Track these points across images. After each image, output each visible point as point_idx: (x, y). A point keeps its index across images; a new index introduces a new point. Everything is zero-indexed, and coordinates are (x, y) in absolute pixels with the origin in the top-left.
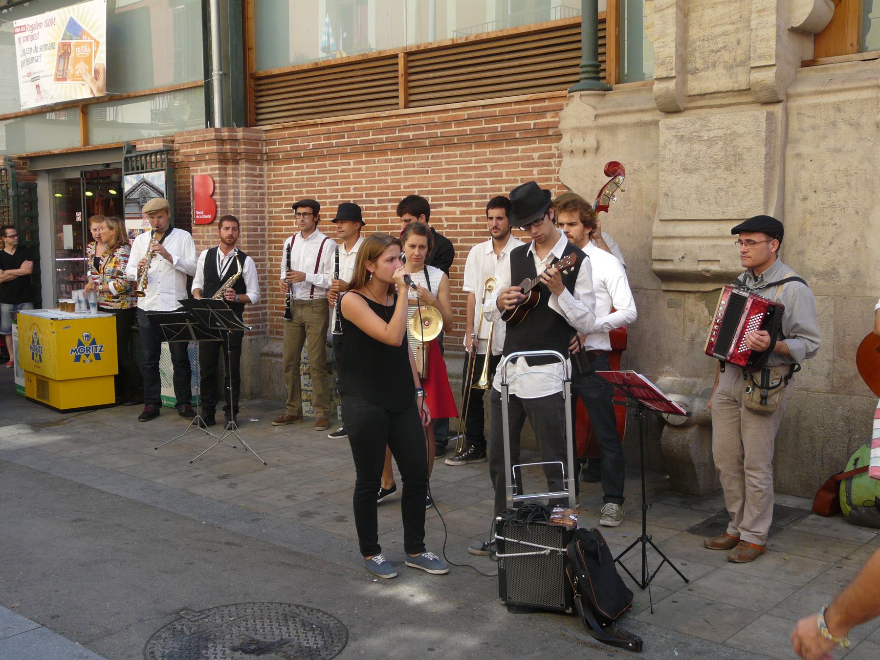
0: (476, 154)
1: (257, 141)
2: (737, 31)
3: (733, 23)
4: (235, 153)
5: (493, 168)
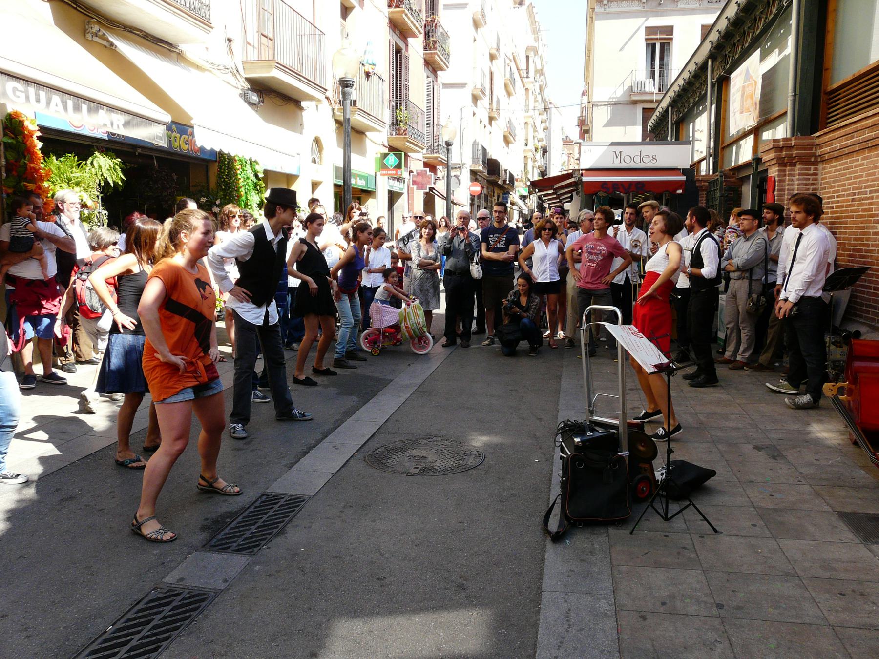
1: (811, 146)
4: (790, 157)
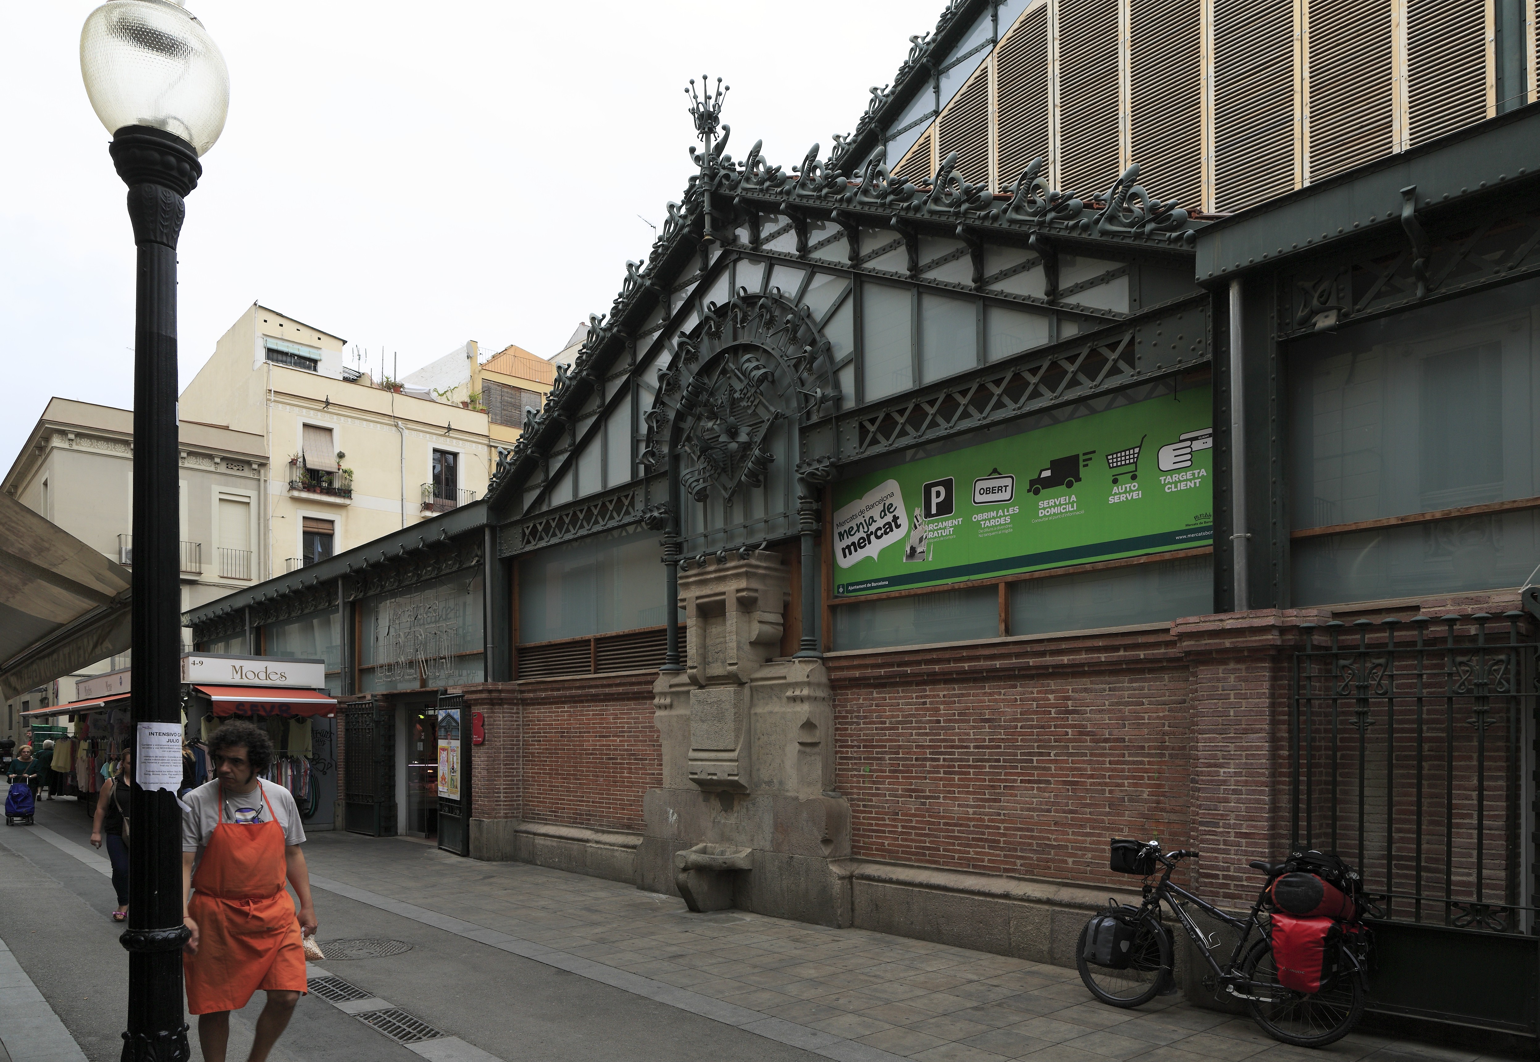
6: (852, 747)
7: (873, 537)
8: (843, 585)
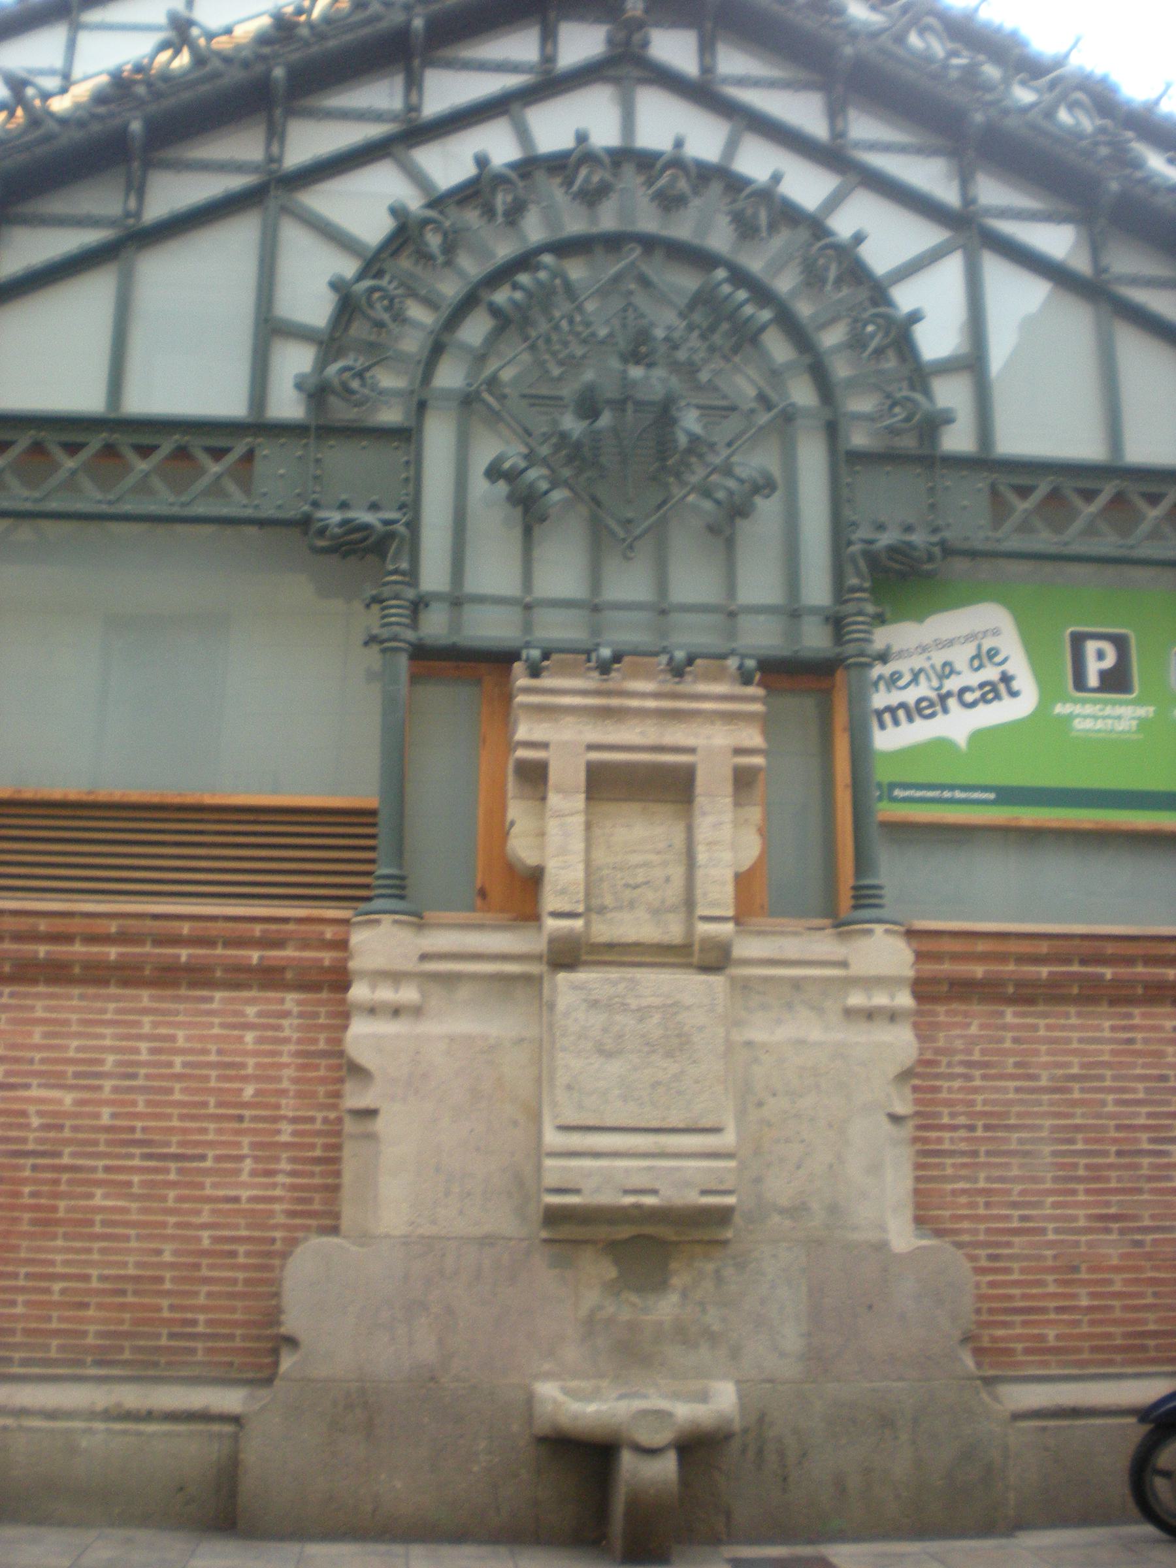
0: (117, 998)
2: (665, 864)
3: (659, 853)
5: (155, 1025)
6: (954, 1128)
7: (952, 703)
8: (879, 786)
